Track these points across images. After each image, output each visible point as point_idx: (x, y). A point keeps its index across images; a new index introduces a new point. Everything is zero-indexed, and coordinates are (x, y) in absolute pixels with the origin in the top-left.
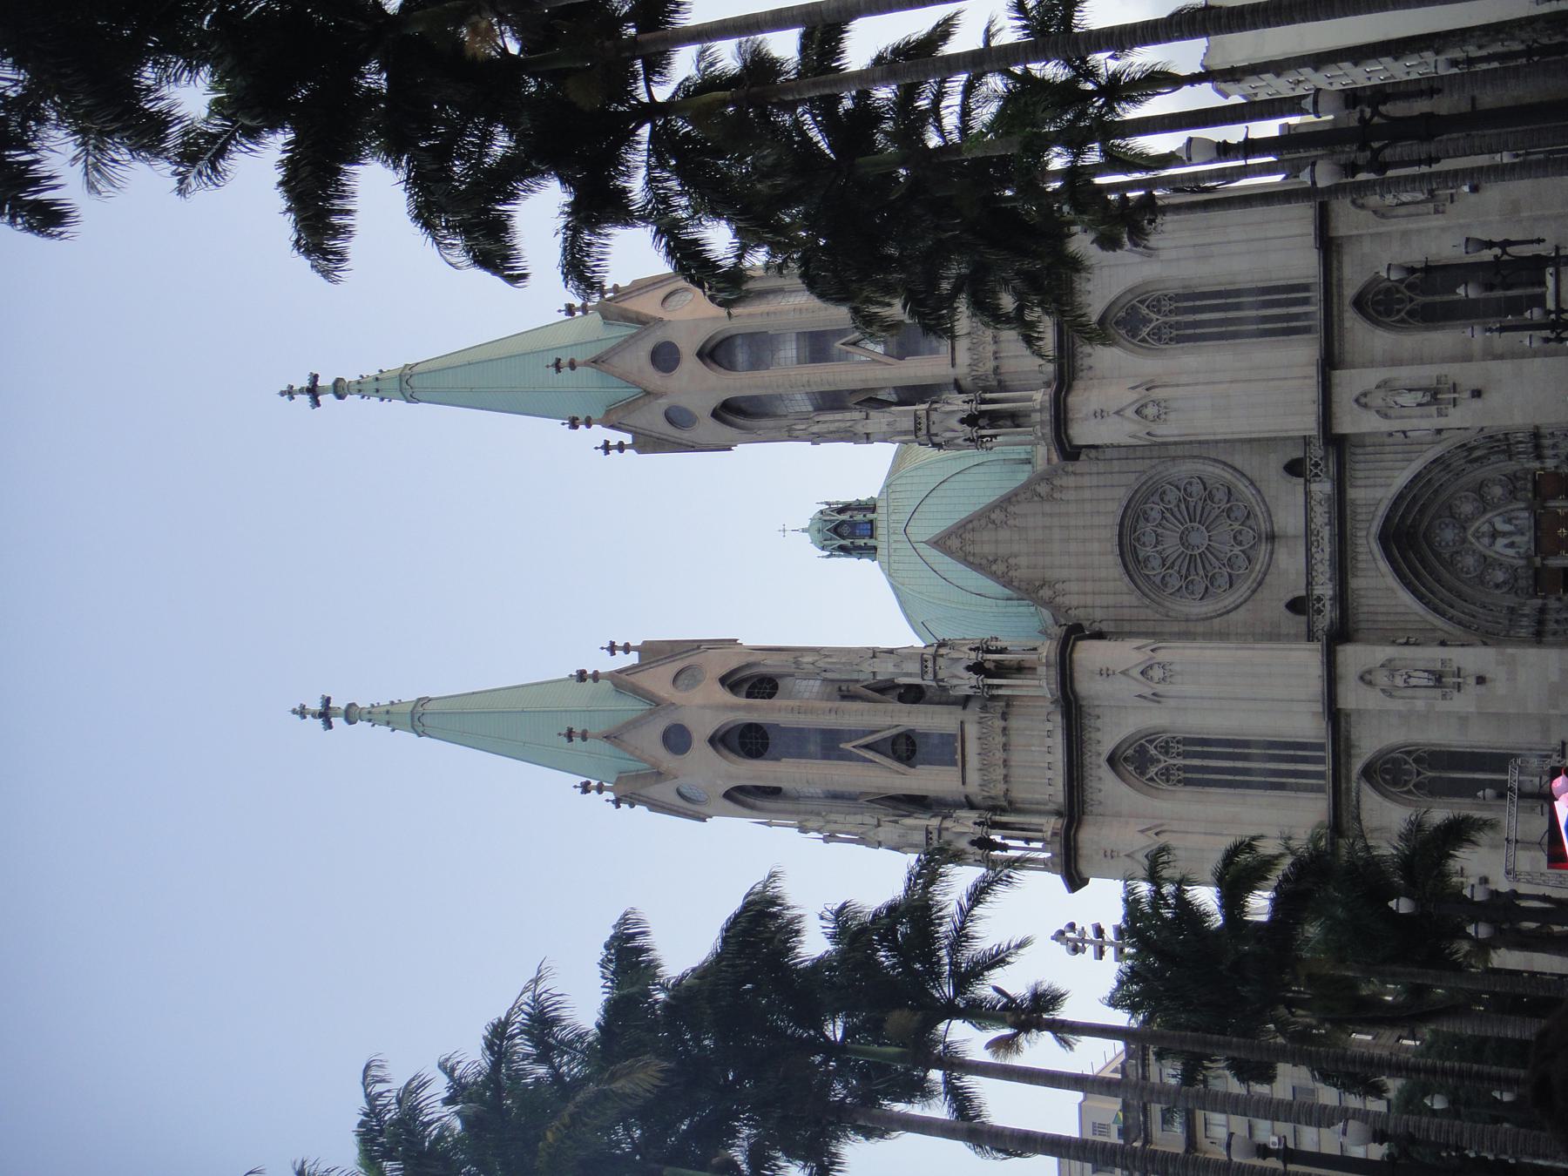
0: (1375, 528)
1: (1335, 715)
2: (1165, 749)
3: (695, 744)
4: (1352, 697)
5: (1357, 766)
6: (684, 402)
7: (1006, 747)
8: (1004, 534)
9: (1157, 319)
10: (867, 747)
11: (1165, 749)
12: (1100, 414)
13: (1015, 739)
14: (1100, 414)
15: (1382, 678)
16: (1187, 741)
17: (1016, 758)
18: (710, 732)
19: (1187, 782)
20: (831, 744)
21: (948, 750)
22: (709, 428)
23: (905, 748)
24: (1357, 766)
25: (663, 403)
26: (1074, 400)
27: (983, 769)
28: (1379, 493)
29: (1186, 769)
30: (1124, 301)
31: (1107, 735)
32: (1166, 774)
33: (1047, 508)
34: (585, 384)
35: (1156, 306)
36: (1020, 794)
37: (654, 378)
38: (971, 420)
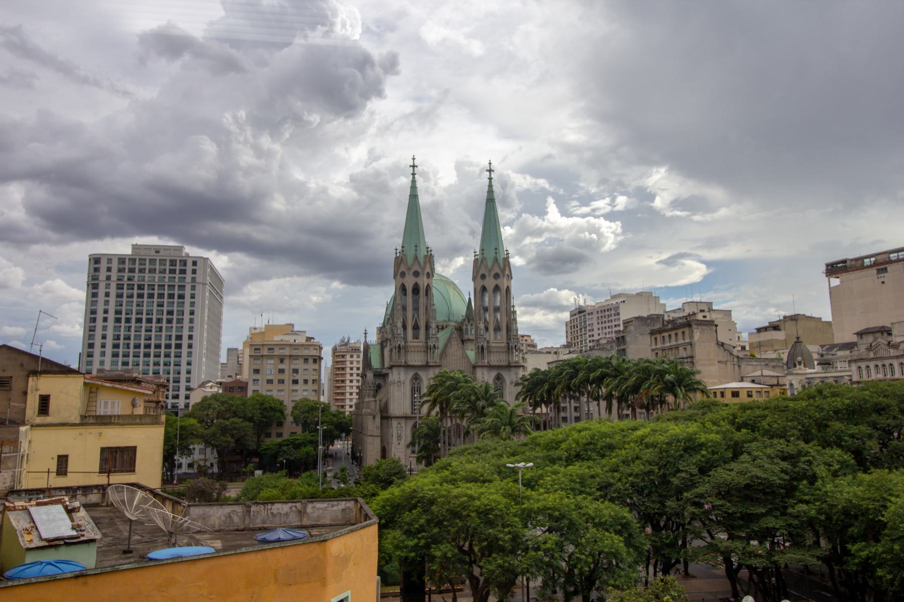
2: (418, 383)
6: (487, 278)
8: (456, 347)
9: (499, 383)
11: (418, 383)
12: (483, 374)
14: (483, 374)
17: (416, 354)
20: (416, 309)
21: (416, 337)
22: (481, 283)
23: (416, 327)
25: (487, 275)
26: (485, 369)
27: (413, 346)
31: (422, 374)
32: (414, 384)
34: (490, 256)
35: (501, 383)
36: (409, 354)
37: (493, 273)
38: (482, 347)
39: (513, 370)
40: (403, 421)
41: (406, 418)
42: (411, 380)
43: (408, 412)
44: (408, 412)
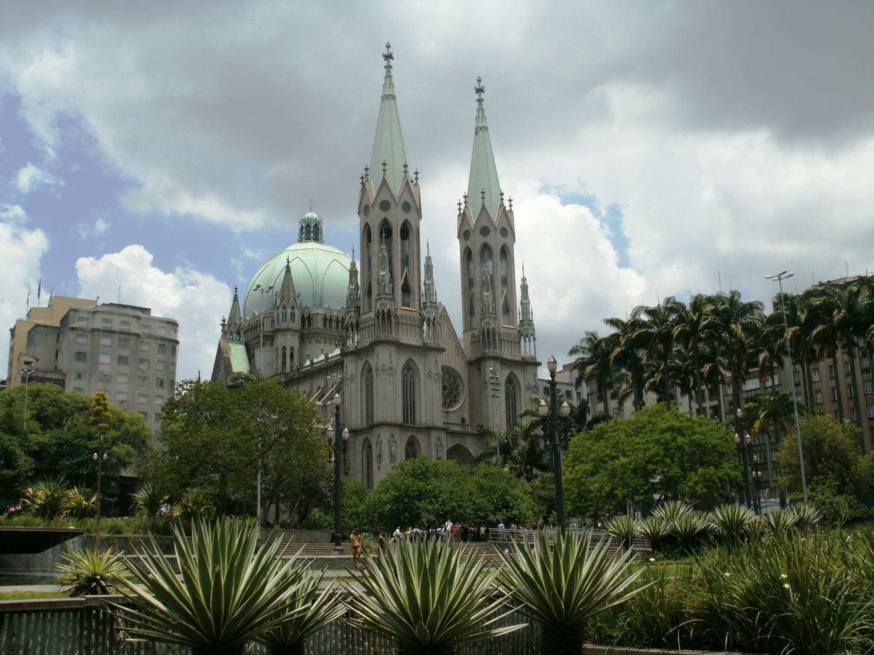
0: (461, 443)
1: (428, 429)
2: (412, 376)
3: (406, 214)
4: (434, 435)
5: (415, 434)
7: (411, 325)
10: (406, 277)
11: (412, 376)
13: (413, 328)
15: (438, 443)
16: (414, 382)
18: (410, 220)
19: (403, 382)
23: (406, 289)
24: (415, 434)
28: (468, 444)
29: (407, 382)
30: (515, 381)
31: (418, 360)
33: (453, 345)
39: (530, 368)
40: (397, 432)
41: (400, 426)
42: (403, 371)
43: (400, 419)
44: (400, 419)
